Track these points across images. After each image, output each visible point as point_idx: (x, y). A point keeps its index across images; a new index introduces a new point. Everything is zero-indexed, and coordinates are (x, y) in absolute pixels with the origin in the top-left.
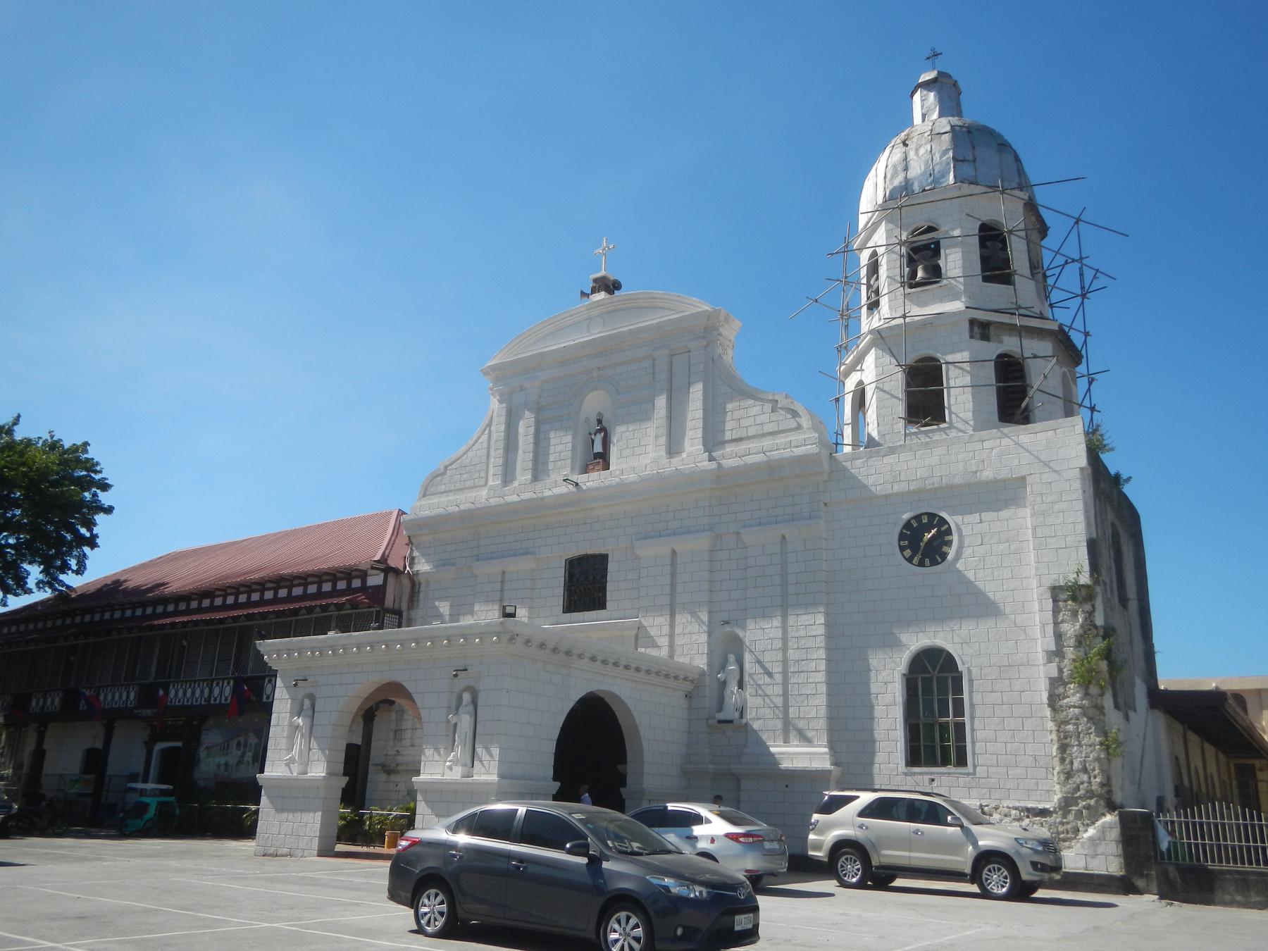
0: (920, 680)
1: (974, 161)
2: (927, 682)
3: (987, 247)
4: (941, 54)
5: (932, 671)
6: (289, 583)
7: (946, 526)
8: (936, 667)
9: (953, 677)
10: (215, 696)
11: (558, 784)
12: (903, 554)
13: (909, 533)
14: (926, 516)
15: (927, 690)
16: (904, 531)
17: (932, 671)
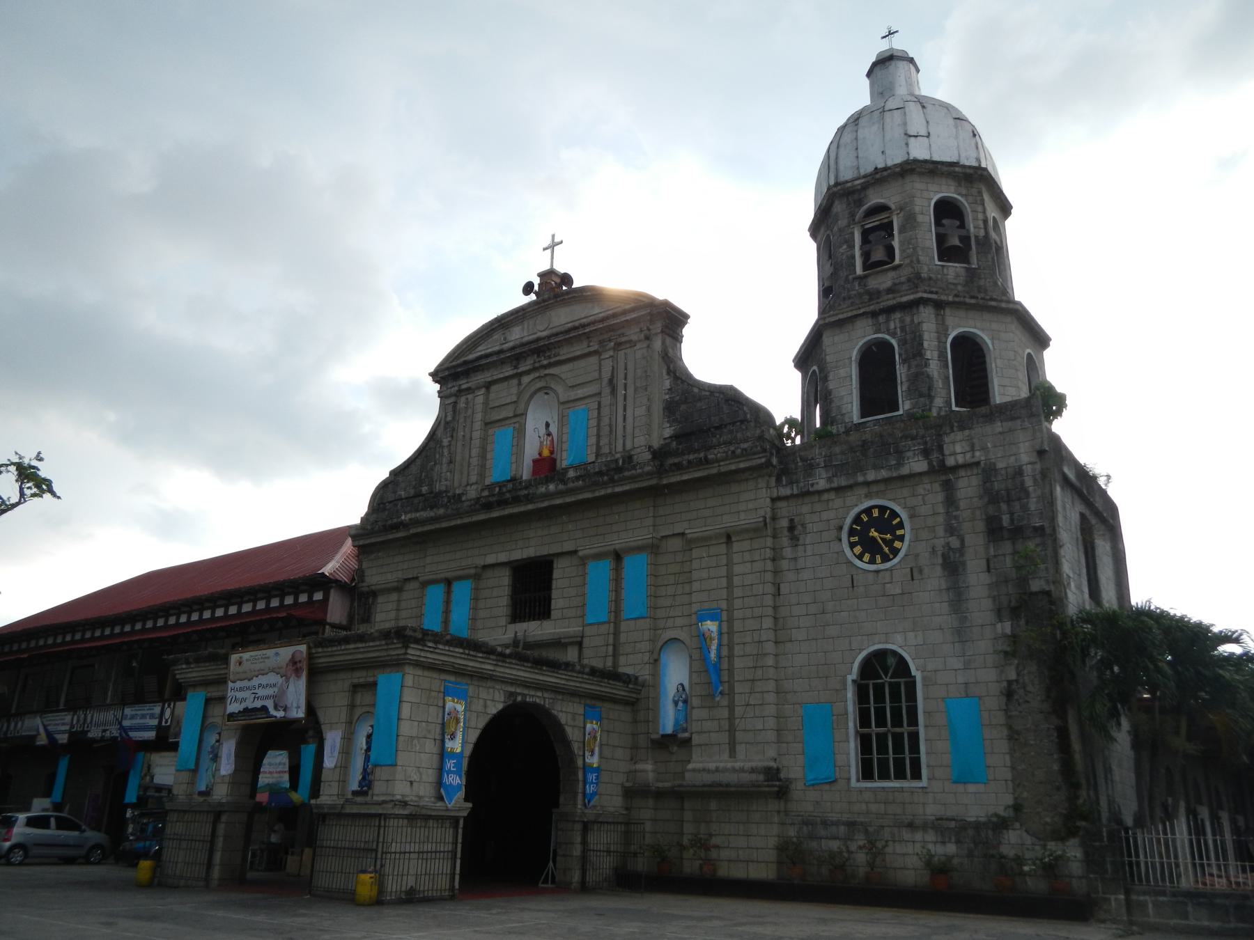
0: (871, 687)
1: (928, 136)
2: (879, 690)
3: (943, 226)
4: (897, 32)
5: (884, 676)
6: (239, 600)
7: (898, 520)
8: (888, 672)
9: (906, 683)
10: (167, 718)
11: (470, 805)
12: (853, 551)
13: (859, 528)
14: (877, 510)
15: (880, 698)
16: (854, 526)
17: (884, 676)
